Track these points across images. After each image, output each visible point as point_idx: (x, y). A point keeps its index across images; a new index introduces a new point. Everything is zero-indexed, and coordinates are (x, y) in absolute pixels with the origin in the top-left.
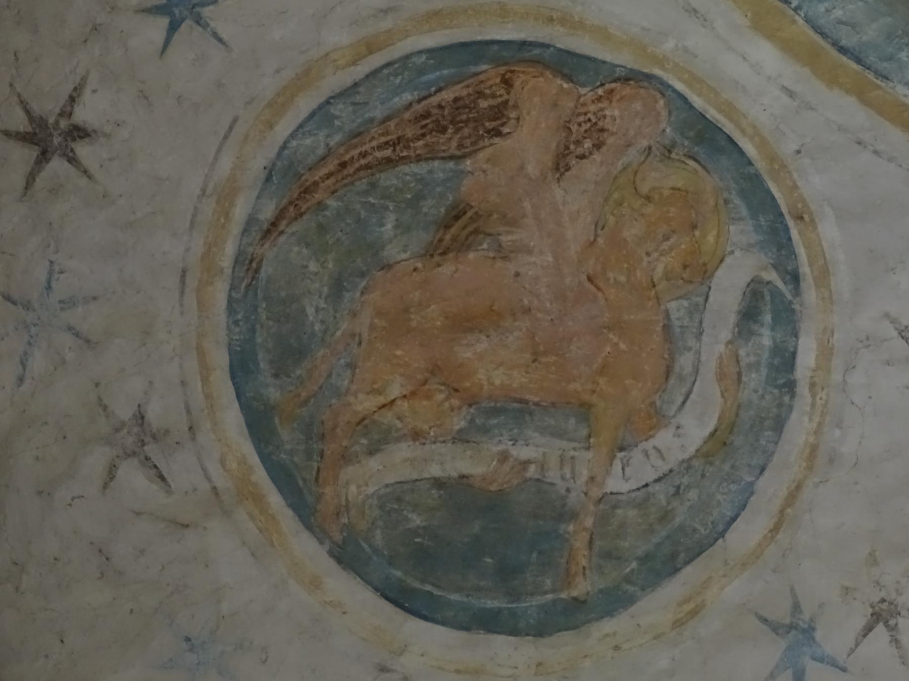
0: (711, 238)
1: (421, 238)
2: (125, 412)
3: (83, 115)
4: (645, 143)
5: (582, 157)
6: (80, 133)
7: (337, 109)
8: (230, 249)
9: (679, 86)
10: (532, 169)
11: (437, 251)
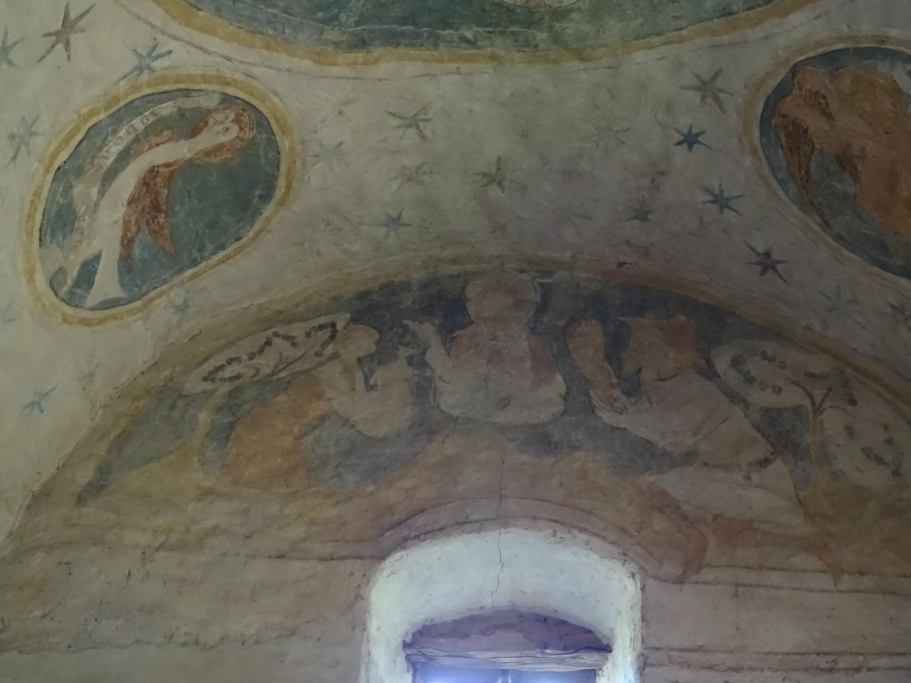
0: (881, 81)
1: (847, 176)
2: (889, 310)
3: (761, 249)
4: (827, 81)
5: (828, 105)
6: (767, 255)
7: (780, 175)
8: (830, 240)
9: (802, 58)
10: (827, 127)
11: (855, 175)
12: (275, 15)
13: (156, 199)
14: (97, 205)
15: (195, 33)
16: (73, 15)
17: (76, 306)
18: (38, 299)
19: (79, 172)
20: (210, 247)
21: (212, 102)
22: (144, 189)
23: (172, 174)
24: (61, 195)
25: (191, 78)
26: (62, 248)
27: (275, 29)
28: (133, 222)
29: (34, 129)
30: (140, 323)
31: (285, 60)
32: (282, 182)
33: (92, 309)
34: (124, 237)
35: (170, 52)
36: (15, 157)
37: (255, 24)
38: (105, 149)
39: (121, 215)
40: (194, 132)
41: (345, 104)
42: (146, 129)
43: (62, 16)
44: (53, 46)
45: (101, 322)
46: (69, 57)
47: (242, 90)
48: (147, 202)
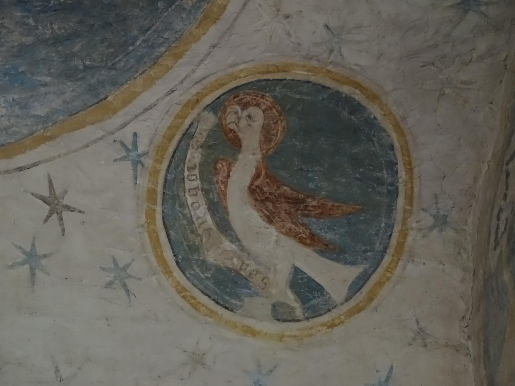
12: (145, 41)
13: (286, 198)
14: (243, 249)
15: (127, 109)
16: (46, 193)
17: (329, 310)
18: (281, 338)
19: (194, 249)
20: (385, 174)
21: (210, 120)
22: (269, 204)
23: (267, 176)
24: (203, 273)
25: (173, 128)
26: (257, 294)
27: (161, 45)
28: (293, 227)
29: (121, 266)
30: (410, 266)
31: (200, 47)
32: (346, 90)
33: (347, 300)
34: (302, 241)
35: (135, 134)
36: (128, 292)
37: (146, 59)
38: (194, 219)
39: (275, 233)
40: (235, 144)
41: (278, 10)
42: (202, 180)
43: (40, 202)
44: (61, 219)
45: (370, 299)
46: (80, 212)
47: (212, 91)
48: (285, 206)
